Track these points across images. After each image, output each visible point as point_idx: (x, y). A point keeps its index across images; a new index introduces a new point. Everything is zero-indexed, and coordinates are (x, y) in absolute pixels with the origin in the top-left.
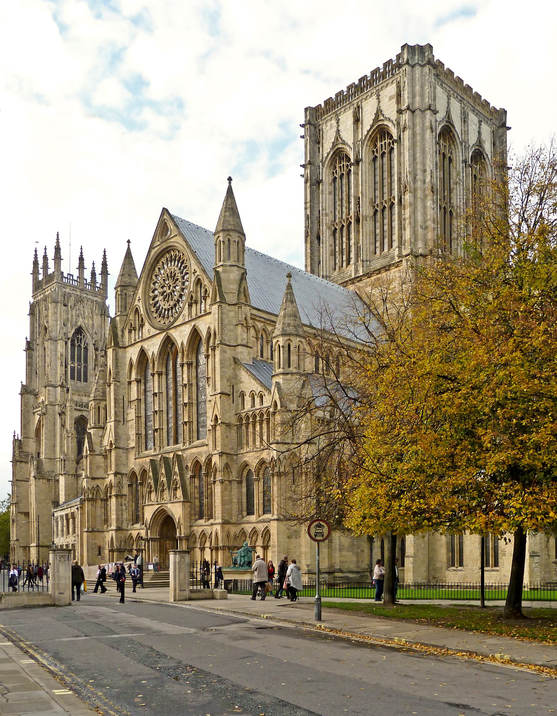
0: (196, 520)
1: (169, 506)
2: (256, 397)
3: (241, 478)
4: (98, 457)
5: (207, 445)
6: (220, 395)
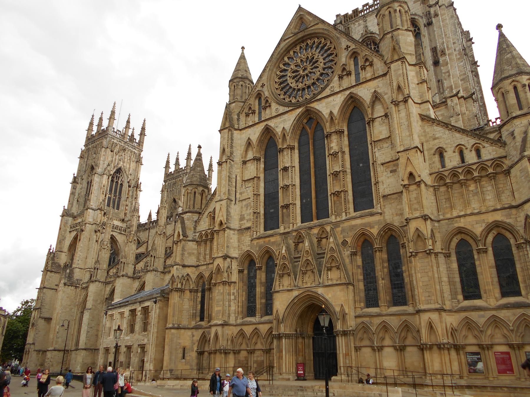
0: (362, 309)
1: (320, 291)
2: (466, 153)
3: (449, 251)
5: (381, 214)
6: (414, 150)
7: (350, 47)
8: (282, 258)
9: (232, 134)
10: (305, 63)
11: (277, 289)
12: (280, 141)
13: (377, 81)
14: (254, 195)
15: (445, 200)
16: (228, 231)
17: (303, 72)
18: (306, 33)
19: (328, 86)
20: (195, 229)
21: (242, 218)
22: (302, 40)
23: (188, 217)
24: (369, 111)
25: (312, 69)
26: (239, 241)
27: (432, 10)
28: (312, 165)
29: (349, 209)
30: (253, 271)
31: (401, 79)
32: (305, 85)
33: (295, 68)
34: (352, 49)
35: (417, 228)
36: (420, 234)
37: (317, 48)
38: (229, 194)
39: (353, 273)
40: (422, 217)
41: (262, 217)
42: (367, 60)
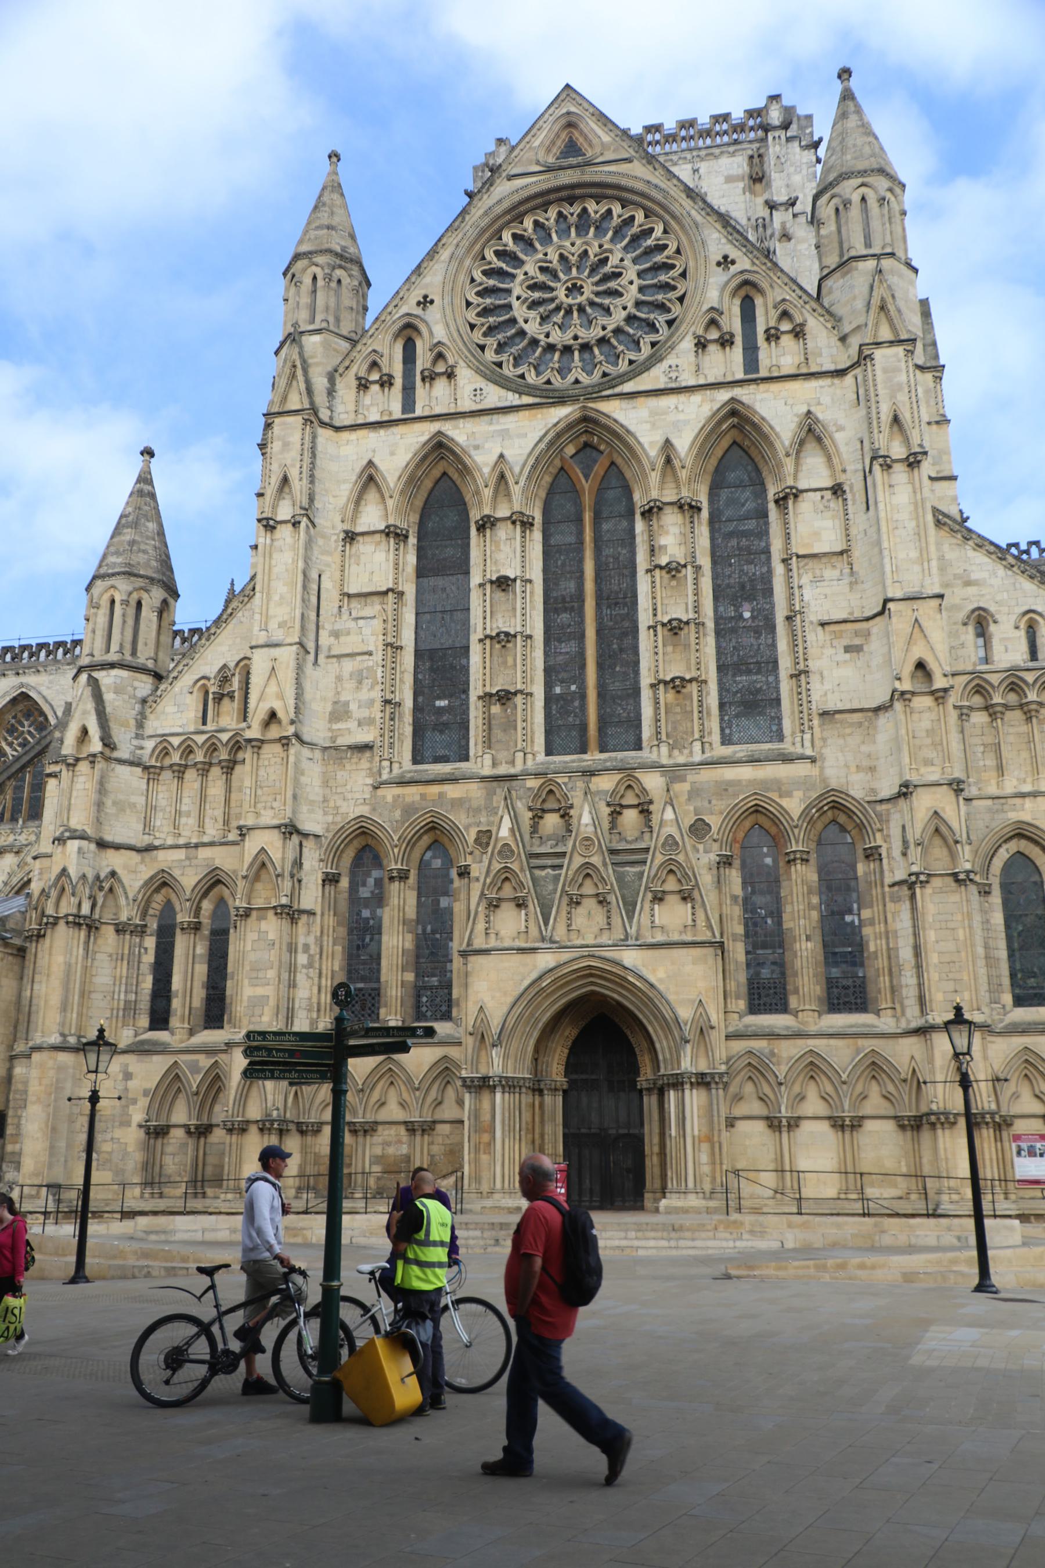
1: (630, 958)
4: (123, 772)
5: (813, 760)
7: (733, 262)
8: (500, 852)
9: (314, 437)
10: (574, 270)
11: (479, 943)
12: (487, 493)
13: (814, 384)
14: (387, 645)
15: (981, 749)
16: (295, 748)
17: (567, 296)
18: (587, 178)
19: (661, 360)
20: (140, 725)
21: (339, 713)
22: (570, 194)
23: (118, 681)
24: (789, 464)
25: (597, 294)
26: (326, 784)
27: (779, 217)
28: (589, 586)
29: (710, 733)
30: (371, 881)
31: (902, 397)
32: (576, 338)
33: (541, 278)
34: (742, 272)
35: (936, 813)
36: (943, 829)
37: (618, 232)
38: (303, 628)
39: (721, 916)
40: (950, 784)
41: (408, 719)
42: (785, 315)
